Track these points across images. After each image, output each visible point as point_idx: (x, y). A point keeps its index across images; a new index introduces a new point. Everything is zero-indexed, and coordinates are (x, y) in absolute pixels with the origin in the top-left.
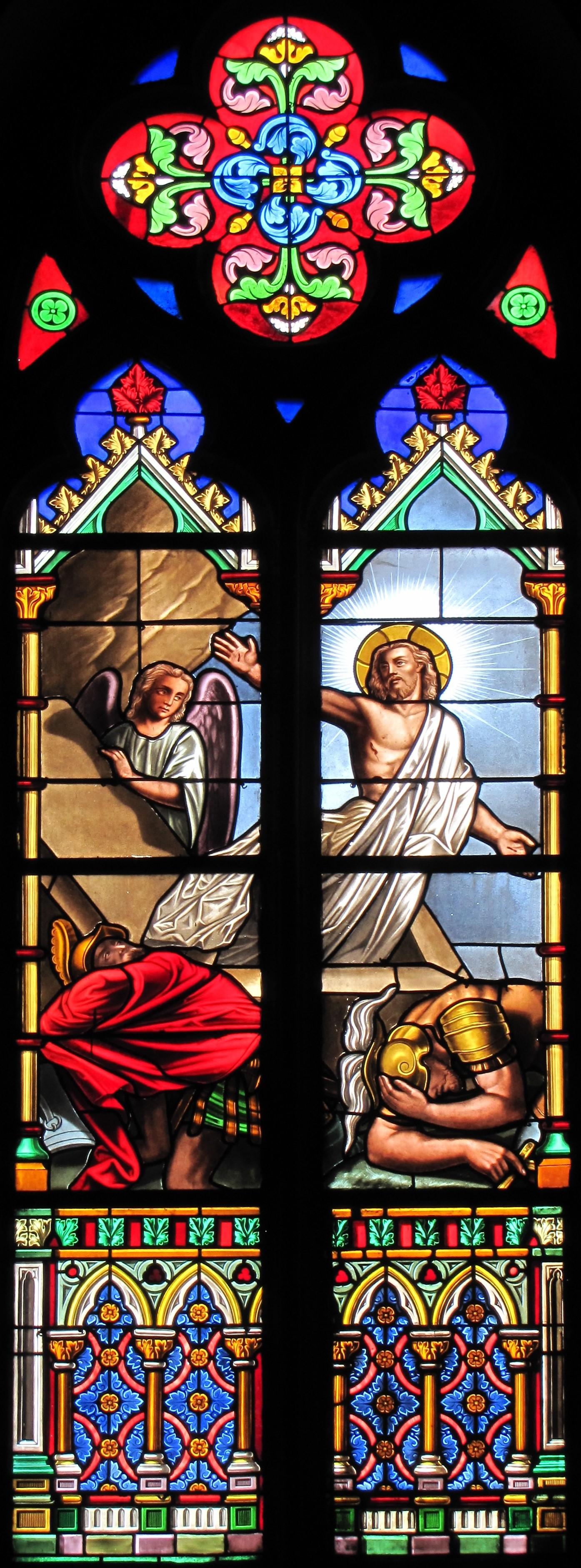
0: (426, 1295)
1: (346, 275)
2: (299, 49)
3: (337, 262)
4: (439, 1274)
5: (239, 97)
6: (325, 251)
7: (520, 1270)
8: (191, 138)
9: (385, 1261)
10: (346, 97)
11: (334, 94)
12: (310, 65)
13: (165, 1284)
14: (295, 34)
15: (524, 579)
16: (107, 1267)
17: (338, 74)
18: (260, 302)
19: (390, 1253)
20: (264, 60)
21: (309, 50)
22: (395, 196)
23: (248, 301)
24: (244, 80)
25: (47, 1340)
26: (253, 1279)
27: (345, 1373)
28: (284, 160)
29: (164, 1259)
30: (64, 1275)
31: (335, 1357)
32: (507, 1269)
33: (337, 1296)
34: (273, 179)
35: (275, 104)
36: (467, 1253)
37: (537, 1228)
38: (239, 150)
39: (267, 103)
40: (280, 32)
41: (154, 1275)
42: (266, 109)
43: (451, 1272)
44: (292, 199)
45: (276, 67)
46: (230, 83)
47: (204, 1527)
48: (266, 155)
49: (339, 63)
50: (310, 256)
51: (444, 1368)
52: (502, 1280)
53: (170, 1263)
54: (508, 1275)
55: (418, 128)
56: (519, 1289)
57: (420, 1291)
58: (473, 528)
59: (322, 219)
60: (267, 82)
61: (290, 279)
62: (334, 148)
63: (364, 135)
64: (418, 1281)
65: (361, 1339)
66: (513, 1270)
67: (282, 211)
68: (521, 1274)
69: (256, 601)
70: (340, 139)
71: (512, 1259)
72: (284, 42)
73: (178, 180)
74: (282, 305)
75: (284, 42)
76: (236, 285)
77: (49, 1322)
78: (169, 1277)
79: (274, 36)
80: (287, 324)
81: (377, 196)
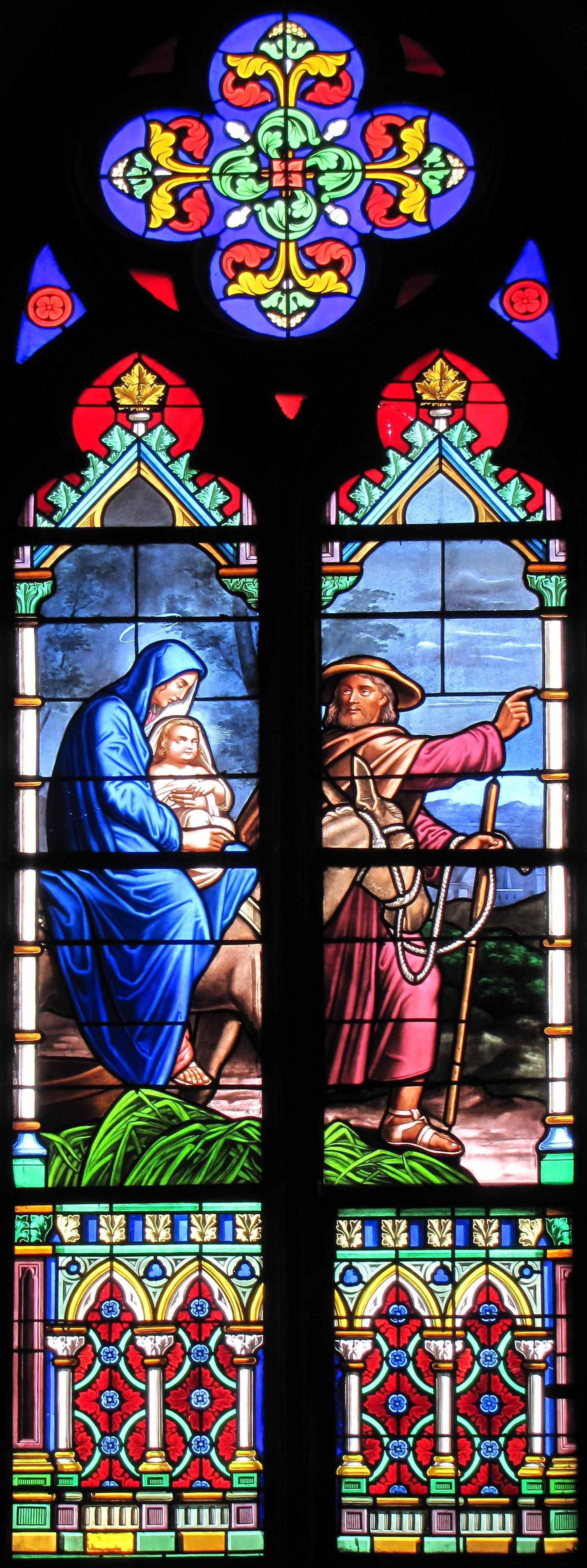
3: (336, 257)
5: (239, 90)
8: (190, 132)
12: (310, 60)
14: (292, 28)
26: (253, 1275)
42: (265, 103)
46: (230, 79)
50: (309, 251)
61: (288, 274)
78: (169, 1274)
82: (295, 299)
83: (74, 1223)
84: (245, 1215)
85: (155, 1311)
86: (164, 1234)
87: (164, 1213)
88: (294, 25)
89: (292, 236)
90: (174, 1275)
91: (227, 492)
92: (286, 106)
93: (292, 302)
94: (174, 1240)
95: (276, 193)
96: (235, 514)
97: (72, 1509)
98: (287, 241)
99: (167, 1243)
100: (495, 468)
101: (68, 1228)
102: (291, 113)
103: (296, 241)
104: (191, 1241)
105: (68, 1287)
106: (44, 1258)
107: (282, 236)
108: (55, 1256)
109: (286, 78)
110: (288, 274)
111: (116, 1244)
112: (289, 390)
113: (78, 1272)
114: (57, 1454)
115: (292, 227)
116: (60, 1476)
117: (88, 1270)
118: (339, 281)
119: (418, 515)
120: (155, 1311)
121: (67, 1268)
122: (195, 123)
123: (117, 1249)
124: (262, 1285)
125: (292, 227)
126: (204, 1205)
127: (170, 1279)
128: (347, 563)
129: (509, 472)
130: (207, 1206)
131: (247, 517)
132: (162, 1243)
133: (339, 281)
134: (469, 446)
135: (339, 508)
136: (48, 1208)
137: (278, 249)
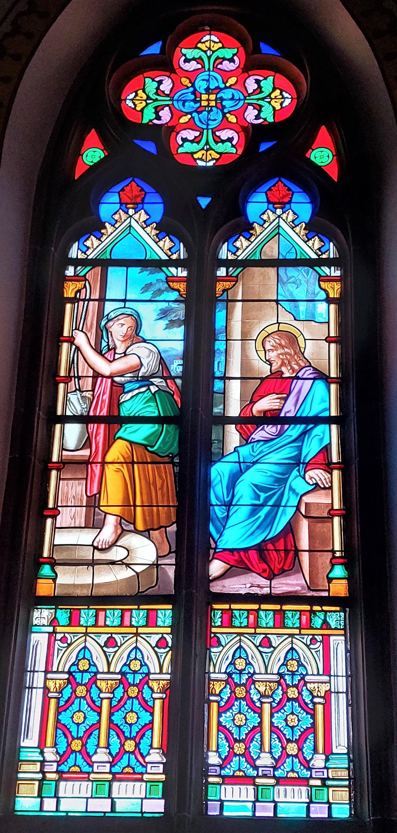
1: (234, 142)
2: (216, 44)
3: (231, 137)
5: (187, 64)
10: (237, 65)
11: (232, 64)
14: (214, 38)
16: (84, 638)
17: (234, 55)
18: (192, 153)
20: (199, 48)
21: (220, 45)
22: (259, 108)
23: (187, 153)
24: (189, 57)
25: (46, 679)
38: (186, 87)
39: (200, 66)
40: (207, 38)
42: (199, 69)
45: (205, 52)
46: (183, 58)
49: (235, 51)
55: (271, 78)
58: (294, 258)
60: (200, 58)
61: (207, 143)
69: (183, 291)
70: (233, 83)
72: (209, 42)
74: (203, 155)
75: (209, 42)
76: (182, 146)
80: (205, 163)
81: (250, 108)
82: (210, 155)
86: (117, 622)
89: (210, 127)
91: (172, 241)
92: (209, 70)
93: (208, 155)
95: (204, 109)
98: (208, 129)
102: (212, 73)
103: (212, 129)
104: (131, 626)
106: (49, 633)
107: (205, 127)
108: (55, 632)
109: (209, 58)
110: (207, 143)
111: (90, 626)
114: (45, 750)
115: (210, 122)
116: (46, 764)
117: (73, 642)
118: (232, 147)
122: (167, 78)
123: (90, 630)
125: (210, 122)
128: (231, 276)
132: (115, 627)
133: (232, 147)
135: (228, 250)
137: (203, 133)
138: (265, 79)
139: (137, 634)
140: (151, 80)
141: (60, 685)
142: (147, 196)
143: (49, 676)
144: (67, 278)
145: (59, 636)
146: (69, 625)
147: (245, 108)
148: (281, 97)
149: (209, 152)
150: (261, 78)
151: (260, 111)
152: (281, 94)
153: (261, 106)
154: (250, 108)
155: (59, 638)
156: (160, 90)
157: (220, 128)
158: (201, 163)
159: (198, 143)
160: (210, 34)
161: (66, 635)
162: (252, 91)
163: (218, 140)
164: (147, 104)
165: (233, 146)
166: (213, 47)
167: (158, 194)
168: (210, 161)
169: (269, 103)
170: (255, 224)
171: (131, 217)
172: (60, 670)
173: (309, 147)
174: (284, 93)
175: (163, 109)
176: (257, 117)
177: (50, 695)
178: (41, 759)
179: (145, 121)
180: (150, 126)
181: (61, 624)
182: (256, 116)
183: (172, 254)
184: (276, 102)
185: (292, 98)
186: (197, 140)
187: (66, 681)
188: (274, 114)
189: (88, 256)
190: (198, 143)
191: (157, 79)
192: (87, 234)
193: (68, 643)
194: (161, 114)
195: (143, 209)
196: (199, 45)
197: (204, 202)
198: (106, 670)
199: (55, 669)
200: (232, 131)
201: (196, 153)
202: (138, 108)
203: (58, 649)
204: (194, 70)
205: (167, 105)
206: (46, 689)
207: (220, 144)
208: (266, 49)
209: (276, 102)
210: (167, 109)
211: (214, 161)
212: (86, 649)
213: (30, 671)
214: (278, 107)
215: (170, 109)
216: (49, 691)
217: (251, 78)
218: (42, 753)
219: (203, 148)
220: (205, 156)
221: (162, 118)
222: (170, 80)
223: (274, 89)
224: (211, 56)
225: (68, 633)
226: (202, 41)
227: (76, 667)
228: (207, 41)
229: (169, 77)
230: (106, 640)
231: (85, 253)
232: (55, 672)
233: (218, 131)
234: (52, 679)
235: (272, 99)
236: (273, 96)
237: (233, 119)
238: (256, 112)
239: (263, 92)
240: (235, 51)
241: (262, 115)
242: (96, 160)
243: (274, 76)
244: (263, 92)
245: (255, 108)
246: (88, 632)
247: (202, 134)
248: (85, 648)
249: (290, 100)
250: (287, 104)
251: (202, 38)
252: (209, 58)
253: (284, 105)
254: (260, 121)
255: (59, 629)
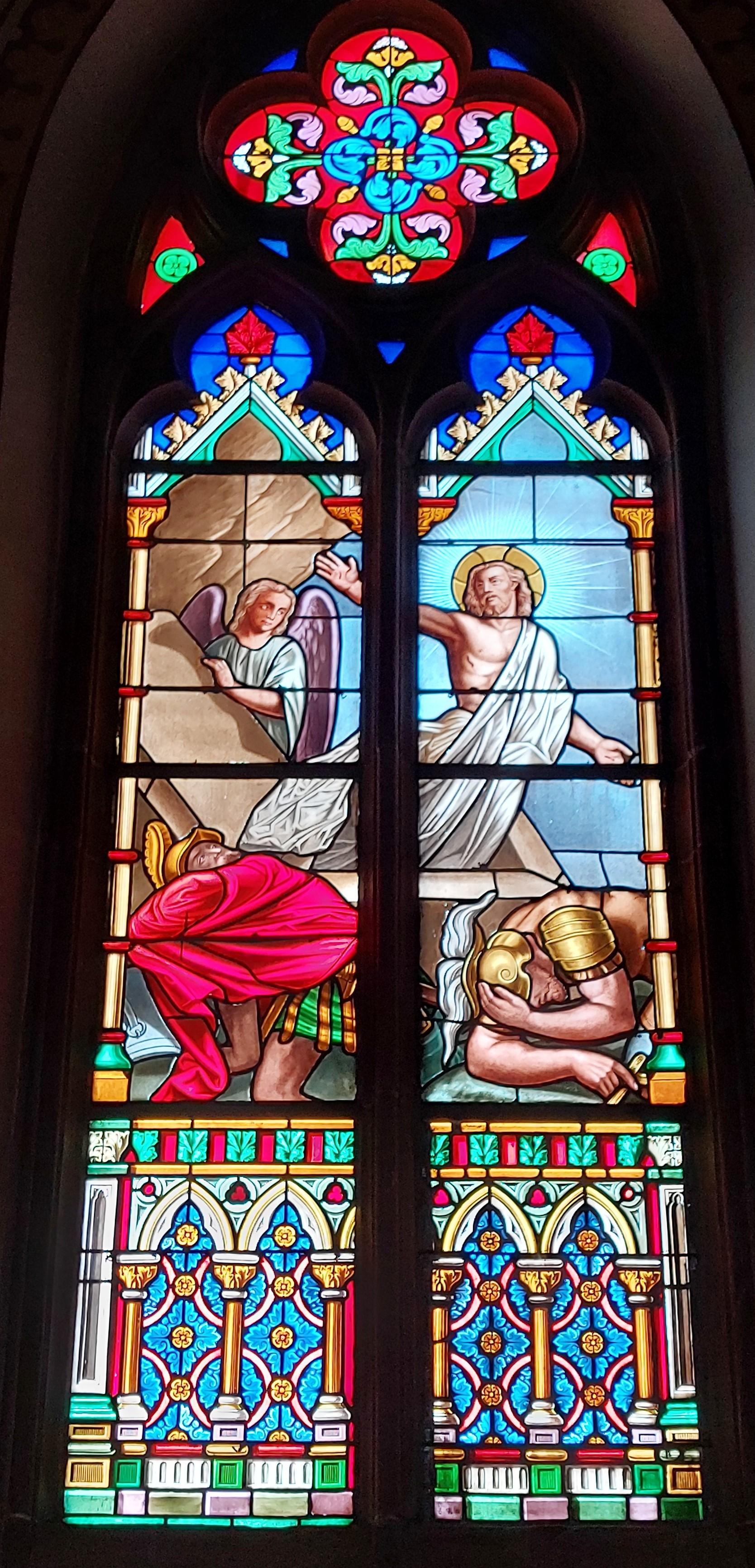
0: (534, 1219)
1: (443, 238)
2: (401, 55)
4: (547, 1196)
5: (348, 92)
6: (426, 216)
7: (635, 1194)
9: (489, 1181)
13: (249, 1204)
15: (613, 505)
17: (435, 74)
18: (365, 260)
19: (494, 1172)
20: (370, 63)
21: (410, 56)
22: (487, 173)
25: (116, 1265)
27: (447, 1306)
28: (388, 143)
29: (247, 1176)
30: (139, 1194)
31: (434, 1289)
32: (622, 1192)
33: (436, 1220)
34: (376, 156)
35: (379, 99)
36: (578, 1173)
37: (652, 1147)
41: (238, 1193)
43: (560, 1195)
44: (395, 175)
45: (382, 69)
47: (285, 1485)
48: (372, 139)
49: (437, 66)
51: (555, 1302)
52: (617, 1204)
53: (255, 1180)
54: (623, 1198)
56: (636, 1215)
57: (527, 1215)
59: (423, 192)
60: (372, 80)
61: (392, 240)
62: (431, 134)
63: (458, 123)
64: (525, 1204)
65: (463, 1268)
66: (629, 1194)
67: (387, 184)
68: (638, 1198)
71: (628, 1180)
73: (293, 157)
77: (121, 1245)
78: (253, 1197)
79: (379, 45)
80: (389, 278)
81: (470, 173)
83: (152, 1139)
84: (337, 1133)
85: (236, 1236)
87: (248, 1130)
88: (397, 39)
90: (258, 1199)
94: (257, 1161)
96: (339, 445)
97: (136, 1464)
98: (392, 213)
99: (249, 1163)
100: (585, 408)
101: (145, 1145)
105: (141, 1211)
110: (392, 240)
112: (390, 339)
113: (154, 1194)
119: (510, 454)
120: (236, 1236)
121: (142, 1189)
122: (310, 118)
123: (197, 1169)
124: (354, 1209)
126: (292, 1121)
127: (254, 1202)
129: (597, 411)
130: (295, 1123)
131: (349, 452)
132: (244, 1163)
134: (560, 389)
136: (126, 1124)
137: (382, 220)
138: (497, 117)
139: (287, 1177)
140: (279, 120)
141: (144, 1275)
142: (281, 339)
143: (123, 1258)
144: (129, 500)
145: (137, 1183)
146: (156, 1161)
147: (459, 173)
148: (527, 150)
149: (395, 259)
150: (488, 116)
151: (489, 179)
152: (528, 144)
153: (490, 170)
154: (470, 173)
155: (139, 1187)
156: (299, 139)
157: (417, 211)
158: (381, 279)
159: (375, 239)
160: (390, 36)
161: (153, 1180)
162: (472, 141)
163: (411, 235)
164: (275, 166)
165: (441, 244)
166: (396, 59)
167: (298, 336)
168: (397, 274)
169: (506, 162)
170: (486, 394)
171: (250, 380)
172: (142, 1248)
173: (584, 245)
174: (534, 143)
175: (304, 175)
176: (486, 190)
177: (126, 1294)
178: (113, 1416)
179: (271, 198)
180: (282, 209)
181: (141, 1160)
182: (482, 188)
183: (330, 450)
184: (518, 160)
185: (549, 153)
186: (373, 234)
187: (156, 1268)
188: (516, 182)
189: (172, 456)
190: (375, 239)
191: (292, 118)
192: (170, 413)
193: (156, 1197)
194: (300, 184)
195: (271, 365)
196: (371, 56)
197: (391, 352)
198: (230, 1247)
199: (132, 1246)
200: (439, 218)
201: (371, 259)
202: (258, 173)
203: (140, 1208)
204: (362, 105)
205: (314, 168)
206: (117, 1284)
207: (415, 242)
208: (499, 60)
209: (518, 160)
210: (312, 174)
211: (407, 274)
212: (191, 1207)
213: (87, 1251)
214: (523, 170)
215: (318, 174)
216: (124, 1287)
217: (470, 115)
218: (114, 1405)
219: (386, 249)
220: (388, 264)
221: (303, 193)
222: (316, 120)
223: (514, 138)
224: (393, 75)
225: (158, 1176)
226: (375, 48)
227: (173, 1239)
228: (384, 48)
229: (314, 115)
230: (228, 1188)
231: (165, 451)
232: (133, 1252)
233: (412, 216)
234: (128, 1265)
235: (511, 154)
236: (512, 148)
237: (439, 193)
238: (482, 181)
239: (493, 143)
240: (437, 66)
241: (493, 185)
242: (181, 273)
243: (513, 112)
244: (493, 143)
245: (478, 173)
246: (194, 1173)
247: (380, 221)
248: (189, 1203)
249: (546, 156)
250: (540, 165)
251: (375, 43)
252: (390, 80)
253: (534, 167)
254: (491, 196)
255: (139, 1169)
